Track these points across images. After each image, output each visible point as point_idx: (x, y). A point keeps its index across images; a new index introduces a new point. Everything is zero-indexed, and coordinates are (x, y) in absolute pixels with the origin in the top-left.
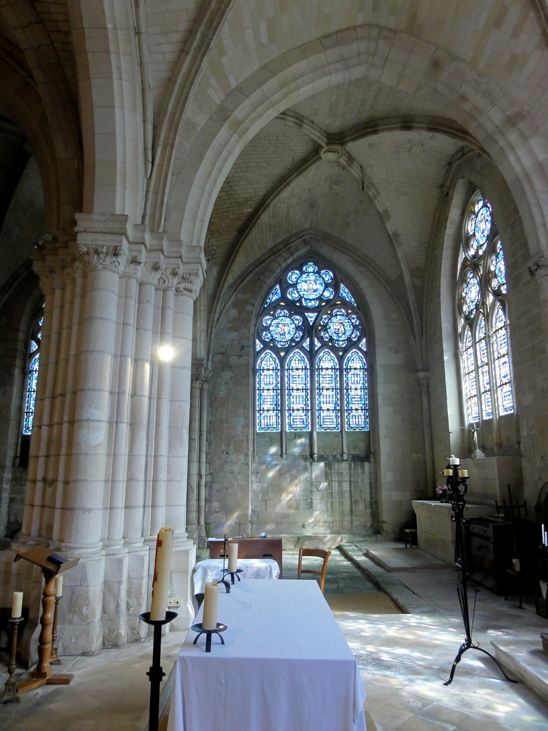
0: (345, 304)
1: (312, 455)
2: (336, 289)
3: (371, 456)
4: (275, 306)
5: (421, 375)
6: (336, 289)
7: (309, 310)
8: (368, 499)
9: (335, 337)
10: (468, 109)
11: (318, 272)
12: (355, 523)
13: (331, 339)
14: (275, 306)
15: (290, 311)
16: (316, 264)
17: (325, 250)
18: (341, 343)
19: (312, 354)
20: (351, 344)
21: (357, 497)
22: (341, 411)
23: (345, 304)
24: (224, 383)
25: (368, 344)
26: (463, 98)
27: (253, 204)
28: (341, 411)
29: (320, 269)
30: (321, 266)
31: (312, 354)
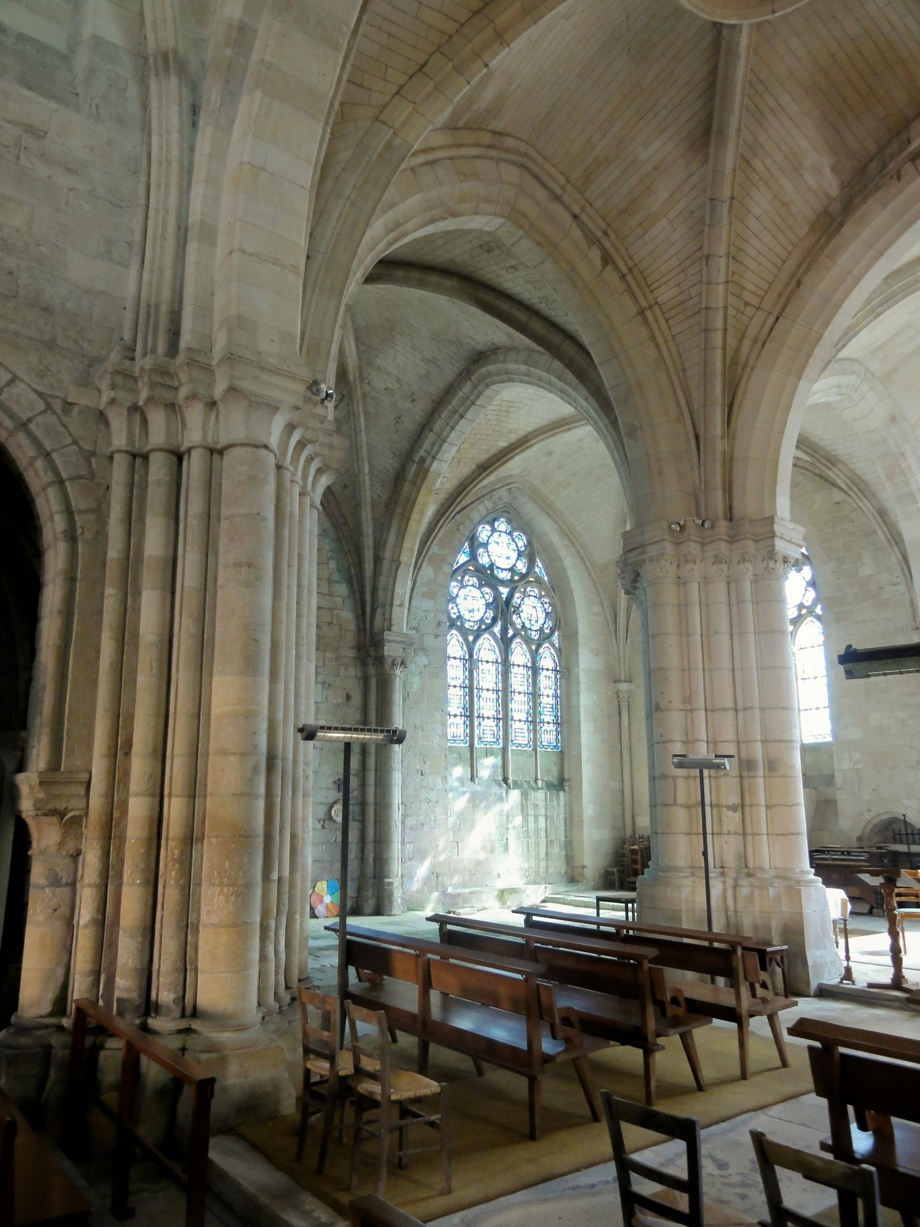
0: (539, 581)
1: (505, 780)
2: (531, 563)
3: (566, 784)
4: (463, 570)
5: (624, 686)
6: (531, 563)
7: (503, 582)
8: (563, 839)
9: (528, 625)
10: (903, 466)
11: (510, 534)
12: (551, 870)
13: (524, 627)
14: (463, 570)
15: (480, 580)
16: (509, 522)
17: (529, 509)
18: (533, 633)
19: (505, 643)
20: (545, 637)
21: (552, 836)
22: (533, 722)
23: (539, 581)
24: (417, 672)
25: (563, 638)
26: (903, 455)
27: (513, 438)
28: (533, 722)
29: (514, 530)
30: (515, 526)
31: (505, 643)
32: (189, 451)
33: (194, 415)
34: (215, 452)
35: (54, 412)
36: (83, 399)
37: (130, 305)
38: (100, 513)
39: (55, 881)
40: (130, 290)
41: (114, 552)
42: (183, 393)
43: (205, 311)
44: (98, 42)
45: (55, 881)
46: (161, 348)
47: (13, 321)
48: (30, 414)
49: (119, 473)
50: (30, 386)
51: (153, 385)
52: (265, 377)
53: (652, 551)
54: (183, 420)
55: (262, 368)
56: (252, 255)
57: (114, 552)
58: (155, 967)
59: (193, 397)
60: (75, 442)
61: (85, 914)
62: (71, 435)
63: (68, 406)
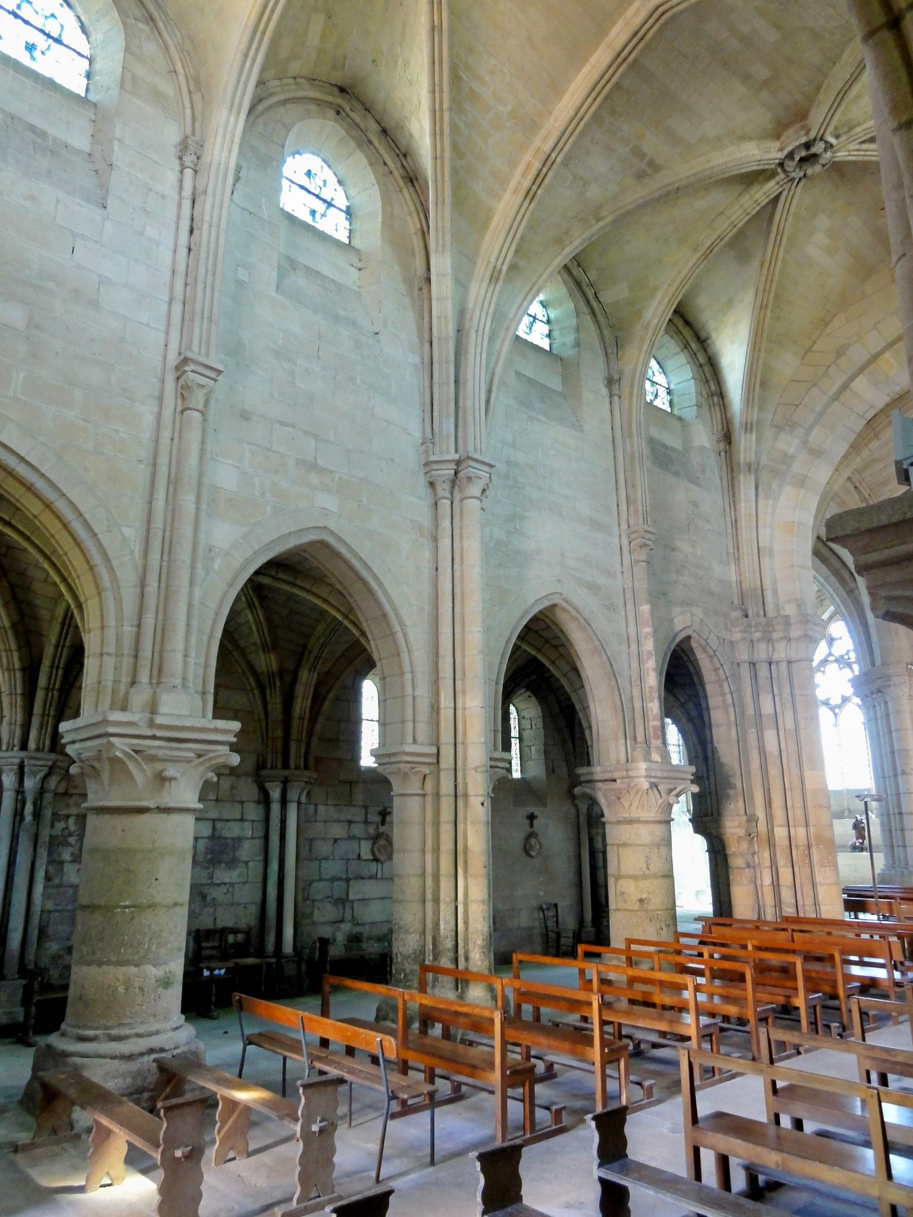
32: (777, 663)
33: (781, 646)
34: (789, 662)
36: (727, 637)
37: (734, 585)
38: (739, 690)
39: (748, 866)
40: (733, 578)
41: (750, 711)
42: (775, 636)
43: (775, 592)
44: (702, 448)
45: (748, 866)
46: (762, 613)
49: (745, 671)
51: (764, 632)
53: (895, 680)
54: (773, 647)
57: (750, 711)
58: (800, 903)
59: (782, 638)
61: (767, 881)
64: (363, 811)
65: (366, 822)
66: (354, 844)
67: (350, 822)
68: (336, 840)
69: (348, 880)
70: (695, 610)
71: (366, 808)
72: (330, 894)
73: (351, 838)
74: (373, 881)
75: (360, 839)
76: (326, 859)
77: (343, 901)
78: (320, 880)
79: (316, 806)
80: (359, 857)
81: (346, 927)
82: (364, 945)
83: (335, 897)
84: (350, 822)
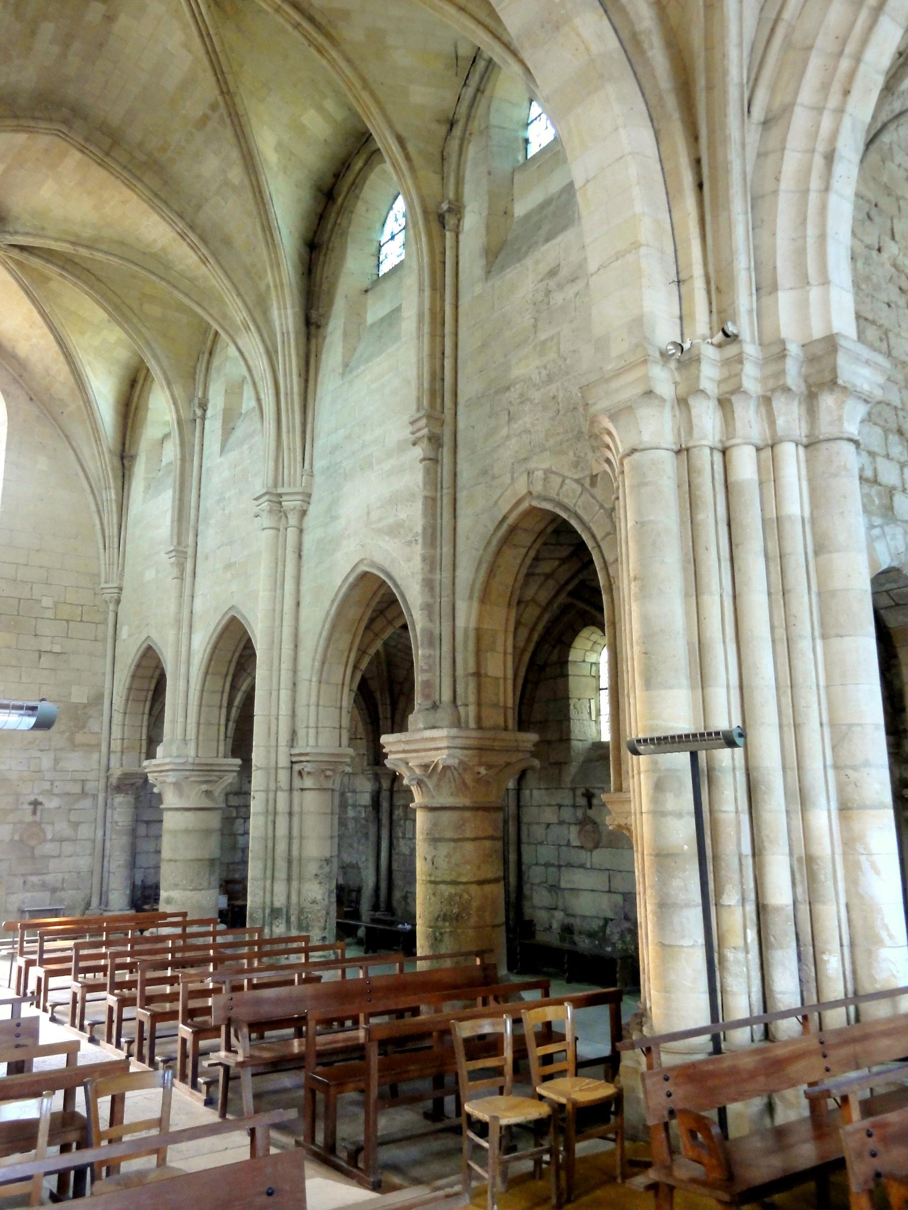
35: (587, 490)
47: (558, 434)
48: (574, 501)
50: (572, 479)
52: (614, 385)
55: (607, 380)
56: (599, 269)
60: (602, 507)
62: (597, 501)
63: (593, 478)
64: (571, 793)
65: (574, 806)
66: (564, 829)
67: (560, 806)
68: (548, 825)
69: (560, 866)
70: (532, 465)
71: (573, 790)
72: (544, 880)
73: (561, 823)
74: (582, 870)
75: (570, 824)
76: (541, 843)
77: (554, 888)
78: (537, 864)
79: (531, 791)
80: (568, 844)
81: (559, 915)
82: (576, 938)
83: (550, 883)
84: (560, 806)
